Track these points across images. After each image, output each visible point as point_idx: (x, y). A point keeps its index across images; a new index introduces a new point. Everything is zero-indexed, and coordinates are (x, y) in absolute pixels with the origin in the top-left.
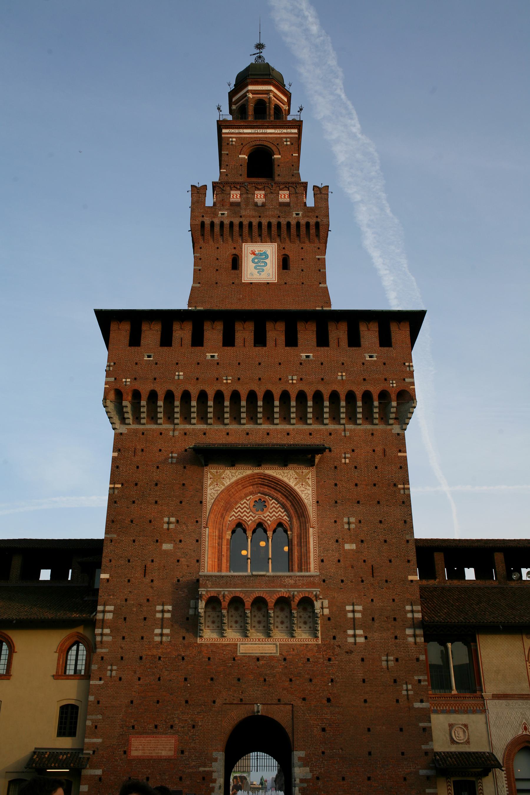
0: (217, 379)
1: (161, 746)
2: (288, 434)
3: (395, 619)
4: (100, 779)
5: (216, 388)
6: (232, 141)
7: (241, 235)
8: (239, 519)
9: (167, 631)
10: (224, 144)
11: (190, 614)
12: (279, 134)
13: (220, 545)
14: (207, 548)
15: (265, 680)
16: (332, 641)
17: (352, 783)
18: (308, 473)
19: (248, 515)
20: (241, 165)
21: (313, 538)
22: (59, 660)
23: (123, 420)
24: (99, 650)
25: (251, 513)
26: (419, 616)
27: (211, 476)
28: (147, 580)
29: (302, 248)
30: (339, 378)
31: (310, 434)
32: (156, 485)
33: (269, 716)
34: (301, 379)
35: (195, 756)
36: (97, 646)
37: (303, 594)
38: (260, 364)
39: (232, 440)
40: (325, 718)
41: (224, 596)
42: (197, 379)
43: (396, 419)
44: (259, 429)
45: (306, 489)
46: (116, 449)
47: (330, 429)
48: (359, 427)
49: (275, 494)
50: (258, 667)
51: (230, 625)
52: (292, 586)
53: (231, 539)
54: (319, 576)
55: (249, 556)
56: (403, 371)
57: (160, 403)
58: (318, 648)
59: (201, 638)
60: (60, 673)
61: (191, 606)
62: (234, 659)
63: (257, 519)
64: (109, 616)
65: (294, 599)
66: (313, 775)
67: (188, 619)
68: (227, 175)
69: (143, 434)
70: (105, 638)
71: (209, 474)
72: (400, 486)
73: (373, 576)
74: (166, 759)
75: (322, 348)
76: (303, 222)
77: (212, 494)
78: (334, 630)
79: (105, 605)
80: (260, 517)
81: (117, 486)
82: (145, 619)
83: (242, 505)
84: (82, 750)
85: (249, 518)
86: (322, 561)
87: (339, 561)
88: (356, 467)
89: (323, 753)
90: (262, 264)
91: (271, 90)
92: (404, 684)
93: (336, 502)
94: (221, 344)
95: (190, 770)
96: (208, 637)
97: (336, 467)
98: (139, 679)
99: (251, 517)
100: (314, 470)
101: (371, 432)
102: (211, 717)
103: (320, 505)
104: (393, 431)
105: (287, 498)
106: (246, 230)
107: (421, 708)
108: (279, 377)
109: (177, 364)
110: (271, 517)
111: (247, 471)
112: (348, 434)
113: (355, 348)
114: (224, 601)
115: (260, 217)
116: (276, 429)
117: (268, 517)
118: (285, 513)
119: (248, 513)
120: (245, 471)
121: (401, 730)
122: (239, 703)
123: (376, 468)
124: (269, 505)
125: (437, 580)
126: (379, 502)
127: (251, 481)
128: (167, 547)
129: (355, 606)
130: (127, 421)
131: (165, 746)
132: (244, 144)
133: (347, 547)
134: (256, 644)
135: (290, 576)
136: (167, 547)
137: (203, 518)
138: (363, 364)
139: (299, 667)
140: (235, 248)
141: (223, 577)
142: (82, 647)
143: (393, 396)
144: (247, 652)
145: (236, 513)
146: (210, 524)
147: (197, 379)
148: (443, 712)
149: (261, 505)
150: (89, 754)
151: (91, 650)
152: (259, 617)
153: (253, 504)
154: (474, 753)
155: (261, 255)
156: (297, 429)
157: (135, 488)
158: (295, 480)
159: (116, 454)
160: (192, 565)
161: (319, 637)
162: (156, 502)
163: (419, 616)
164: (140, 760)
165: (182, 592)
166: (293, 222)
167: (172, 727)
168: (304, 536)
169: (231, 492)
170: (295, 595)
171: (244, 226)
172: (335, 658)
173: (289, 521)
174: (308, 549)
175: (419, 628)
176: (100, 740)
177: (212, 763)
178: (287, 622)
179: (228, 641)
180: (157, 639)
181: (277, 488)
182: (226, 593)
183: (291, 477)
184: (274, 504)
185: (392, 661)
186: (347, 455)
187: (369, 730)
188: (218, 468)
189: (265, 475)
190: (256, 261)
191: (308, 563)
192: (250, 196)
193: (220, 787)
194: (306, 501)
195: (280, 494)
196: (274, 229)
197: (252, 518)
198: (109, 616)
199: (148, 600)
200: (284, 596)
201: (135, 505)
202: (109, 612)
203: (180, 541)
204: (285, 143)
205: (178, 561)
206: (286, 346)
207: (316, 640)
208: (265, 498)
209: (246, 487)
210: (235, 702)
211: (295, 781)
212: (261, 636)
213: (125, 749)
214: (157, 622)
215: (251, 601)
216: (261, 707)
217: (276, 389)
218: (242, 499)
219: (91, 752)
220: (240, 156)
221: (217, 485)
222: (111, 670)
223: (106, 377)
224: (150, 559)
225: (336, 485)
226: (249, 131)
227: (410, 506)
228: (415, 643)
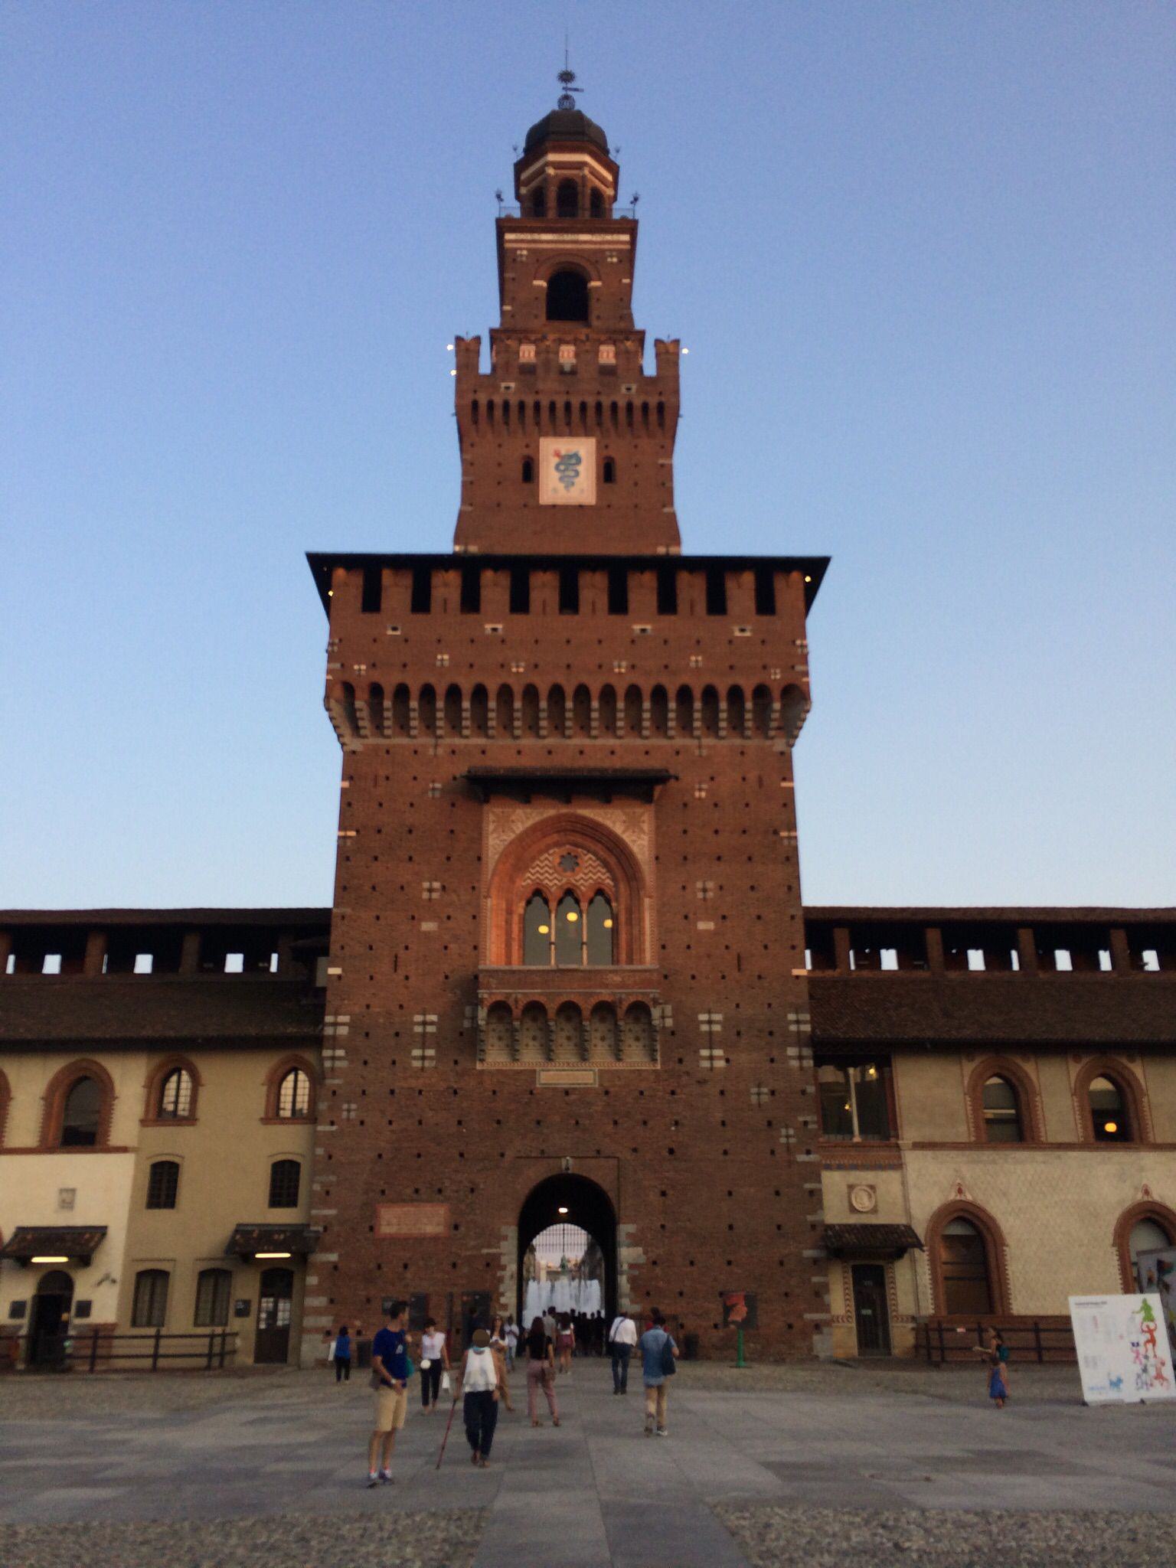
2: (613, 753)
3: (771, 1033)
4: (336, 1268)
5: (500, 681)
6: (521, 255)
7: (538, 424)
8: (538, 883)
9: (430, 1052)
10: (508, 261)
12: (601, 243)
13: (508, 923)
15: (577, 1123)
16: (678, 1066)
18: (642, 814)
23: (356, 729)
24: (328, 1082)
25: (556, 875)
26: (807, 1028)
29: (636, 447)
32: (410, 832)
34: (633, 667)
41: (516, 1001)
42: (471, 666)
43: (779, 728)
46: (347, 775)
48: (722, 742)
54: (657, 970)
55: (553, 939)
57: (414, 704)
62: (531, 1093)
64: (343, 1031)
66: (648, 1259)
67: (461, 1034)
70: (338, 1064)
72: (784, 834)
76: (638, 402)
77: (497, 846)
78: (681, 1050)
79: (336, 1014)
82: (397, 1034)
84: (308, 1225)
86: (663, 947)
87: (689, 947)
88: (716, 805)
91: (585, 164)
93: (685, 858)
94: (507, 609)
95: (468, 1253)
97: (685, 805)
98: (390, 1123)
100: (652, 807)
106: (545, 414)
107: (808, 1162)
112: (705, 752)
115: (568, 393)
117: (582, 881)
119: (551, 874)
121: (777, 1193)
122: (540, 1155)
125: (838, 970)
126: (750, 859)
128: (428, 926)
130: (363, 732)
133: (702, 926)
134: (563, 1070)
136: (428, 926)
138: (730, 642)
140: (527, 446)
141: (513, 972)
142: (302, 1076)
143: (776, 693)
144: (551, 1082)
146: (494, 892)
147: (471, 666)
148: (840, 1167)
153: (558, 860)
155: (570, 457)
157: (378, 836)
159: (346, 784)
160: (466, 953)
162: (411, 859)
163: (807, 1028)
164: (394, 1240)
166: (622, 403)
167: (440, 1191)
169: (524, 843)
171: (542, 410)
175: (806, 1046)
176: (332, 1212)
180: (417, 1064)
182: (519, 996)
187: (730, 1193)
191: (642, 951)
193: (512, 1276)
194: (639, 857)
195: (600, 845)
198: (343, 1031)
199: (401, 1007)
203: (449, 918)
208: (577, 852)
210: (533, 1155)
211: (622, 1266)
212: (574, 1059)
215: (556, 1007)
216: (571, 1161)
218: (541, 852)
219: (321, 1229)
222: (349, 1111)
223: (329, 662)
225: (685, 832)
227: (796, 864)
228: (801, 1068)
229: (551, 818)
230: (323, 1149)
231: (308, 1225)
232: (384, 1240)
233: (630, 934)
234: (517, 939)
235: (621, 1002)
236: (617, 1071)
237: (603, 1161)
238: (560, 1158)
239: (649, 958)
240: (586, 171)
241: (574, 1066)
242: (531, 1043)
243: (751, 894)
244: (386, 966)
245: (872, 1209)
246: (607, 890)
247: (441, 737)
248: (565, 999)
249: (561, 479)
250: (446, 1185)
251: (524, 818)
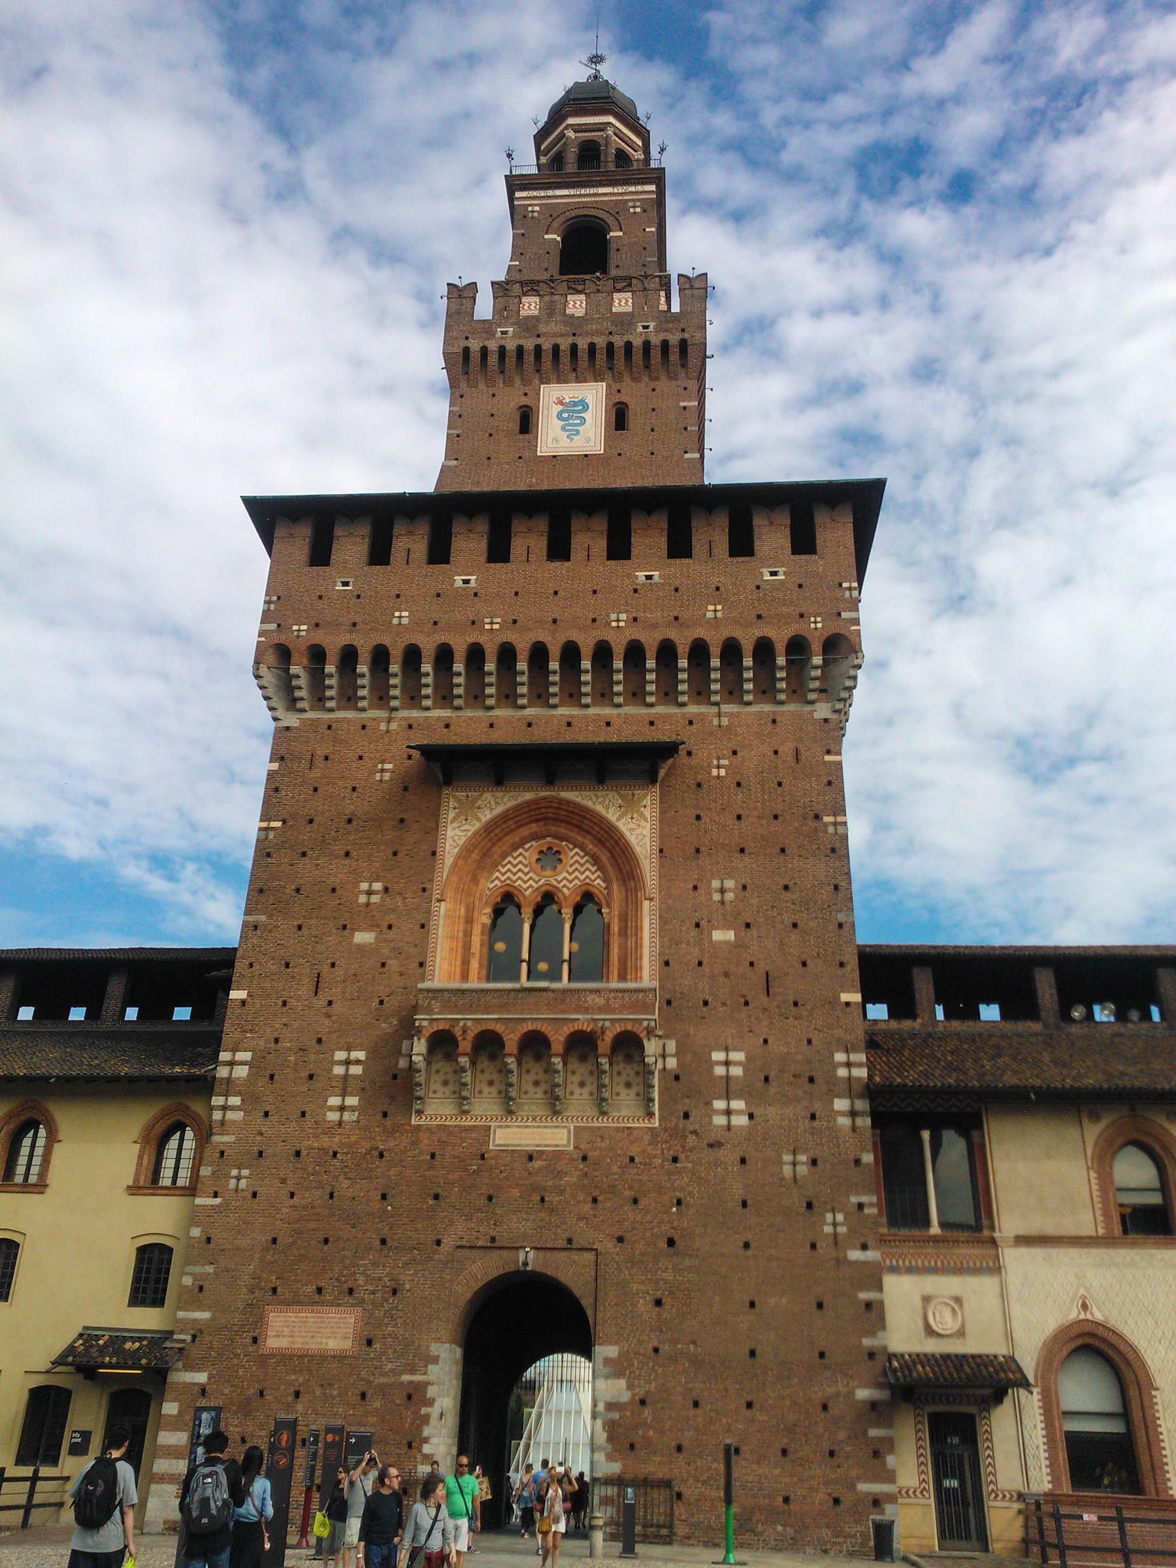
0: (473, 623)
1: (327, 1330)
2: (608, 724)
3: (811, 1080)
5: (471, 639)
8: (508, 885)
9: (352, 1101)
11: (400, 1066)
12: (621, 194)
13: (468, 934)
14: (440, 941)
15: (543, 1200)
16: (682, 1122)
17: (713, 1414)
18: (645, 796)
20: (548, 253)
21: (650, 920)
22: (140, 1157)
23: (292, 703)
24: (216, 1139)
26: (862, 1073)
28: (321, 1002)
29: (654, 390)
30: (710, 615)
31: (652, 723)
32: (350, 821)
33: (549, 1273)
34: (635, 619)
35: (395, 1351)
36: (214, 1131)
37: (623, 1025)
38: (556, 593)
39: (499, 737)
40: (663, 1280)
42: (435, 623)
46: (277, 756)
49: (580, 839)
50: (530, 1173)
51: (477, 1090)
52: (600, 1010)
56: (837, 598)
58: (652, 1135)
60: (142, 1184)
62: (483, 1157)
66: (633, 1395)
67: (395, 1077)
68: (520, 270)
69: (329, 728)
70: (230, 1115)
72: (826, 819)
73: (768, 994)
74: (334, 1357)
75: (678, 561)
76: (656, 340)
77: (456, 838)
78: (686, 1100)
79: (234, 1050)
81: (274, 824)
82: (311, 1077)
83: (515, 858)
84: (172, 1333)
85: (528, 884)
86: (667, 963)
87: (700, 964)
88: (739, 784)
89: (656, 1350)
90: (575, 422)
91: (610, 123)
92: (828, 1211)
93: (698, 851)
95: (383, 1380)
97: (699, 785)
99: (531, 882)
100: (657, 789)
101: (772, 717)
102: (430, 1274)
104: (816, 715)
105: (602, 843)
106: (547, 359)
108: (591, 616)
109: (398, 596)
110: (570, 882)
112: (725, 721)
113: (743, 559)
114: (464, 1039)
115: (574, 335)
117: (565, 882)
118: (598, 873)
121: (820, 1306)
123: (780, 784)
125: (919, 1021)
126: (783, 850)
128: (363, 937)
129: (730, 1054)
131: (335, 1330)
132: (554, 217)
133: (718, 935)
134: (527, 1127)
135: (597, 991)
136: (363, 937)
138: (758, 587)
139: (613, 1174)
140: (526, 394)
143: (816, 647)
145: (503, 874)
147: (435, 623)
148: (910, 1270)
149: (550, 857)
150: (184, 1341)
151: (204, 1136)
153: (536, 856)
154: (973, 1356)
155: (575, 404)
159: (275, 766)
161: (654, 1114)
162: (347, 854)
164: (285, 1357)
166: (637, 342)
167: (351, 1291)
170: (608, 1028)
171: (543, 354)
172: (687, 1157)
173: (605, 889)
176: (206, 1315)
177: (426, 1366)
180: (333, 1116)
181: (584, 826)
185: (803, 1163)
186: (724, 762)
187: (752, 1305)
189: (561, 801)
190: (565, 415)
191: (638, 969)
192: (556, 298)
194: (638, 849)
196: (601, 356)
197: (534, 885)
198: (241, 1072)
199: (319, 1041)
200: (584, 1029)
201: (306, 860)
202: (242, 1063)
203: (390, 927)
204: (632, 210)
205: (383, 965)
206: (609, 558)
208: (561, 846)
209: (522, 826)
210: (480, 1243)
213: (255, 1335)
214: (334, 1084)
215: (516, 1038)
216: (532, 1255)
217: (586, 639)
219: (188, 1338)
220: (546, 237)
221: (466, 820)
222: (238, 1178)
223: (262, 622)
224: (329, 961)
225: (698, 818)
226: (565, 192)
228: (854, 1128)
229: (528, 804)
230: (199, 1229)
231: (172, 1333)
232: (272, 1355)
233: (624, 948)
234: (477, 954)
235: (603, 1033)
236: (599, 1128)
237: (575, 1256)
238: (517, 1248)
239: (648, 976)
240: (610, 132)
241: (542, 1122)
242: (486, 1089)
243: (786, 895)
244: (305, 990)
245: (958, 1331)
247: (396, 709)
248: (530, 1027)
249: (563, 429)
250: (360, 1282)
251: (493, 803)
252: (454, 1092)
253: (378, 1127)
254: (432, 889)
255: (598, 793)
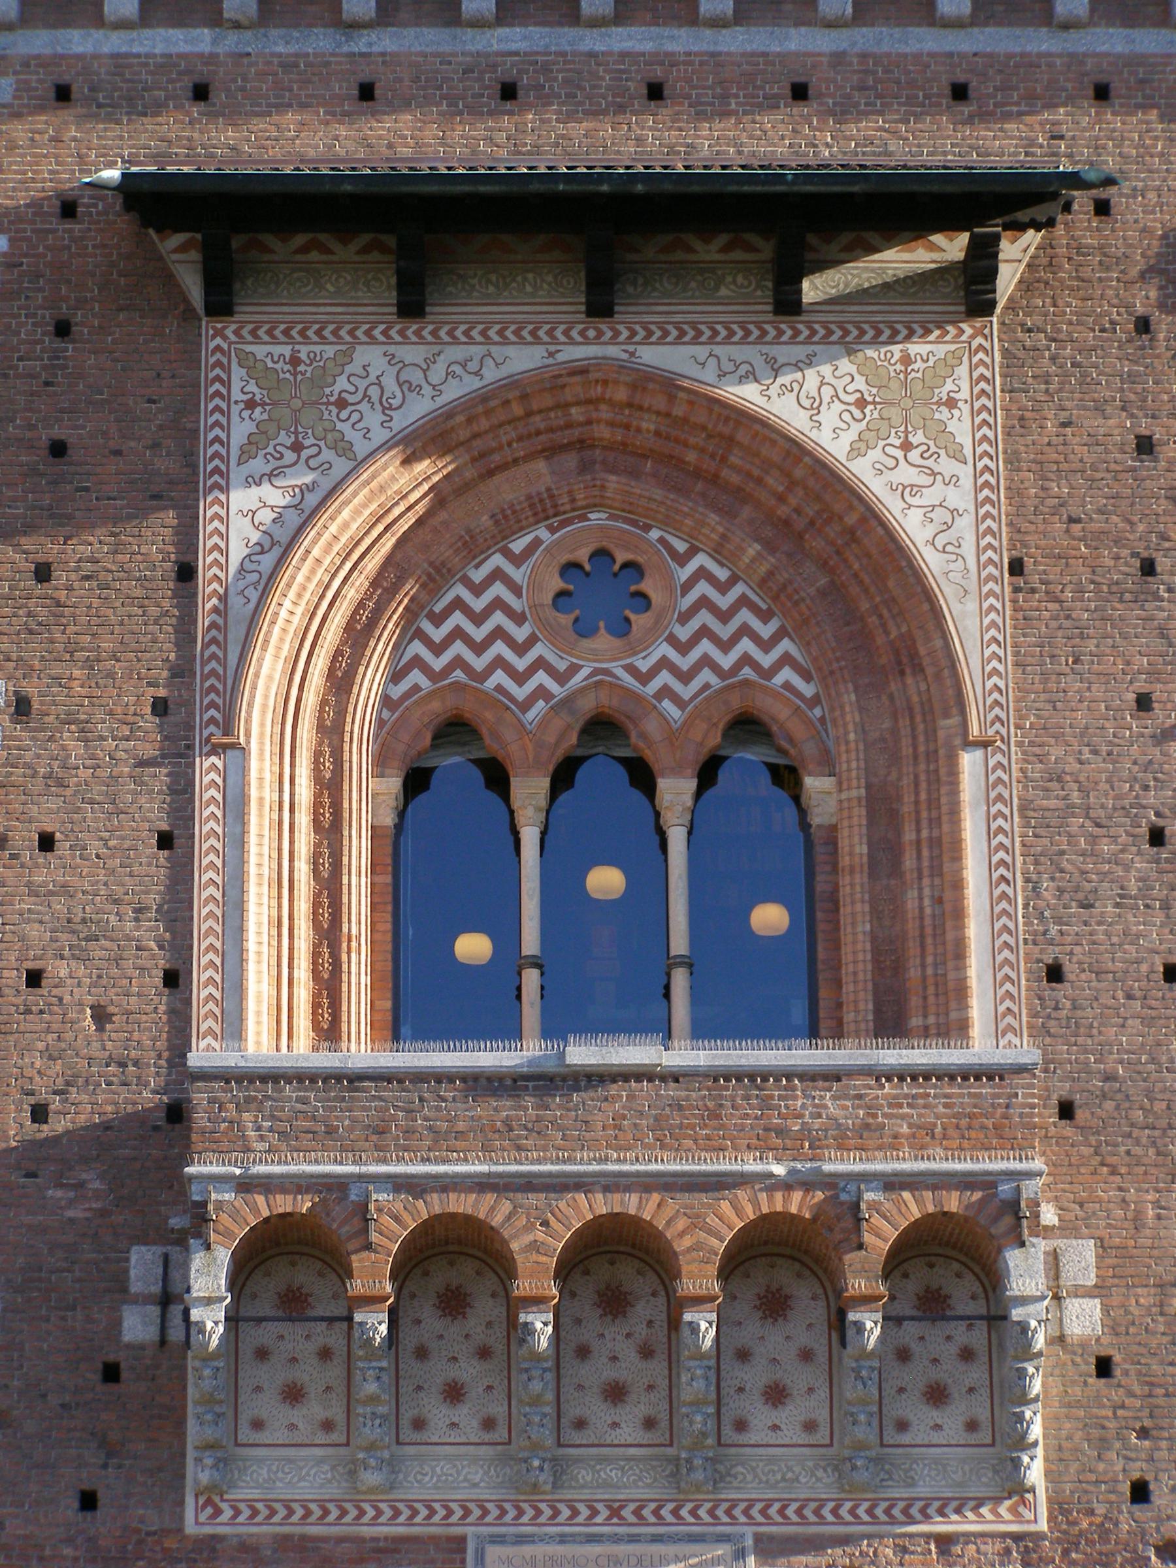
8: (457, 686)
11: (127, 1337)
16: (1127, 1518)
18: (949, 365)
19: (521, 664)
27: (252, 387)
44: (592, 55)
45: (934, 474)
47: (1096, 55)
51: (407, 1416)
53: (399, 827)
59: (209, 1502)
61: (135, 1287)
63: (582, 691)
65: (858, 1230)
67: (111, 1373)
71: (238, 373)
80: (606, 672)
86: (1055, 974)
96: (255, 1494)
99: (541, 677)
103: (1033, 591)
110: (685, 677)
111: (511, 351)
116: (713, 55)
119: (521, 649)
120: (494, 349)
124: (671, 589)
127: (538, 422)
135: (833, 1076)
137: (205, 678)
141: (354, 1079)
145: (438, 649)
152: (614, 1358)
153: (556, 583)
156: (864, 56)
158: (857, 414)
161: (1032, 1490)
165: (71, 1194)
168: (917, 803)
173: (815, 701)
174: (948, 895)
178: (811, 1390)
179: (401, 1519)
183: (827, 392)
184: (703, 588)
188: (302, 333)
194: (931, 561)
203: (47, 843)
205: (34, 979)
207: (1013, 1510)
209: (503, 467)
221: (297, 447)
225: (1145, 446)
242: (439, 1414)
246: (778, 712)
252: (328, 1426)
253: (69, 1541)
254: (189, 703)
255: (774, 350)
